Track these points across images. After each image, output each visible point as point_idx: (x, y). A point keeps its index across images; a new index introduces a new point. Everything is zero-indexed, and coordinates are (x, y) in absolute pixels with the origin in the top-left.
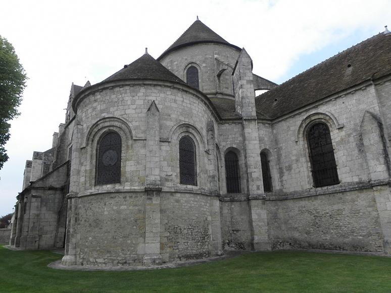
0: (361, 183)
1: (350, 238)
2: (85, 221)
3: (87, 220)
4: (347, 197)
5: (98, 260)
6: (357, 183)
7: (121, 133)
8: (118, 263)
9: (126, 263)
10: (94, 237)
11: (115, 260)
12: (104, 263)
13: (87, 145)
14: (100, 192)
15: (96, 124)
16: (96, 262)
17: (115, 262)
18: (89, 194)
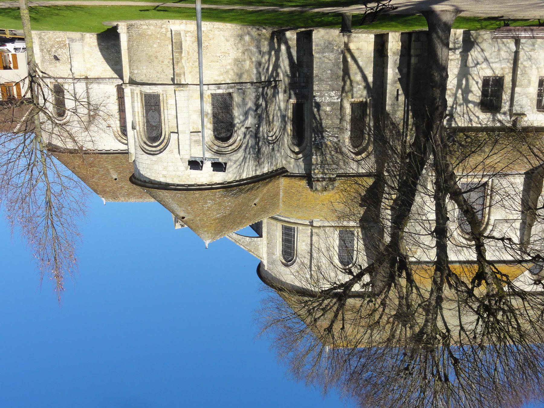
0: (98, 83)
1: (110, 44)
2: (163, 62)
3: (160, 62)
4: (109, 74)
5: (145, 27)
6: (100, 83)
7: (145, 140)
8: (134, 26)
9: (131, 26)
10: (151, 47)
11: (136, 28)
12: (142, 25)
13: (169, 135)
14: (148, 86)
15: (161, 151)
16: (147, 26)
17: (136, 26)
18: (158, 86)
